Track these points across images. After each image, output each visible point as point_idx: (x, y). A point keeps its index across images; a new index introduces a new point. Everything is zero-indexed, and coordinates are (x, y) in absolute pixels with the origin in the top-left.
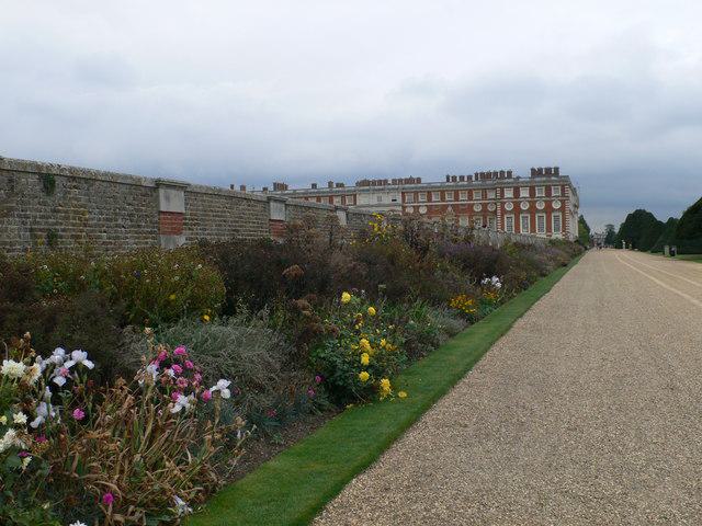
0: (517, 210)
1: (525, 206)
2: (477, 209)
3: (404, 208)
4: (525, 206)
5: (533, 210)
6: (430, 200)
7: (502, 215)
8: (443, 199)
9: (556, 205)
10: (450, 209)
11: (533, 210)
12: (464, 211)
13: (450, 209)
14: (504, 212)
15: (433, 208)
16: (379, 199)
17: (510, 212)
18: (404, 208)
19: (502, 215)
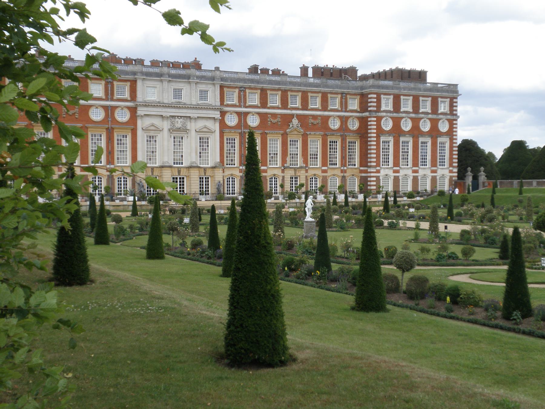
0: (397, 131)
1: (406, 126)
2: (335, 124)
3: (223, 114)
4: (406, 126)
5: (416, 132)
6: (264, 103)
7: (378, 137)
8: (284, 104)
9: (444, 127)
10: (295, 121)
11: (416, 132)
12: (314, 127)
13: (295, 121)
14: (380, 132)
15: (270, 119)
16: (178, 93)
17: (389, 133)
18: (223, 114)
19: (378, 137)
